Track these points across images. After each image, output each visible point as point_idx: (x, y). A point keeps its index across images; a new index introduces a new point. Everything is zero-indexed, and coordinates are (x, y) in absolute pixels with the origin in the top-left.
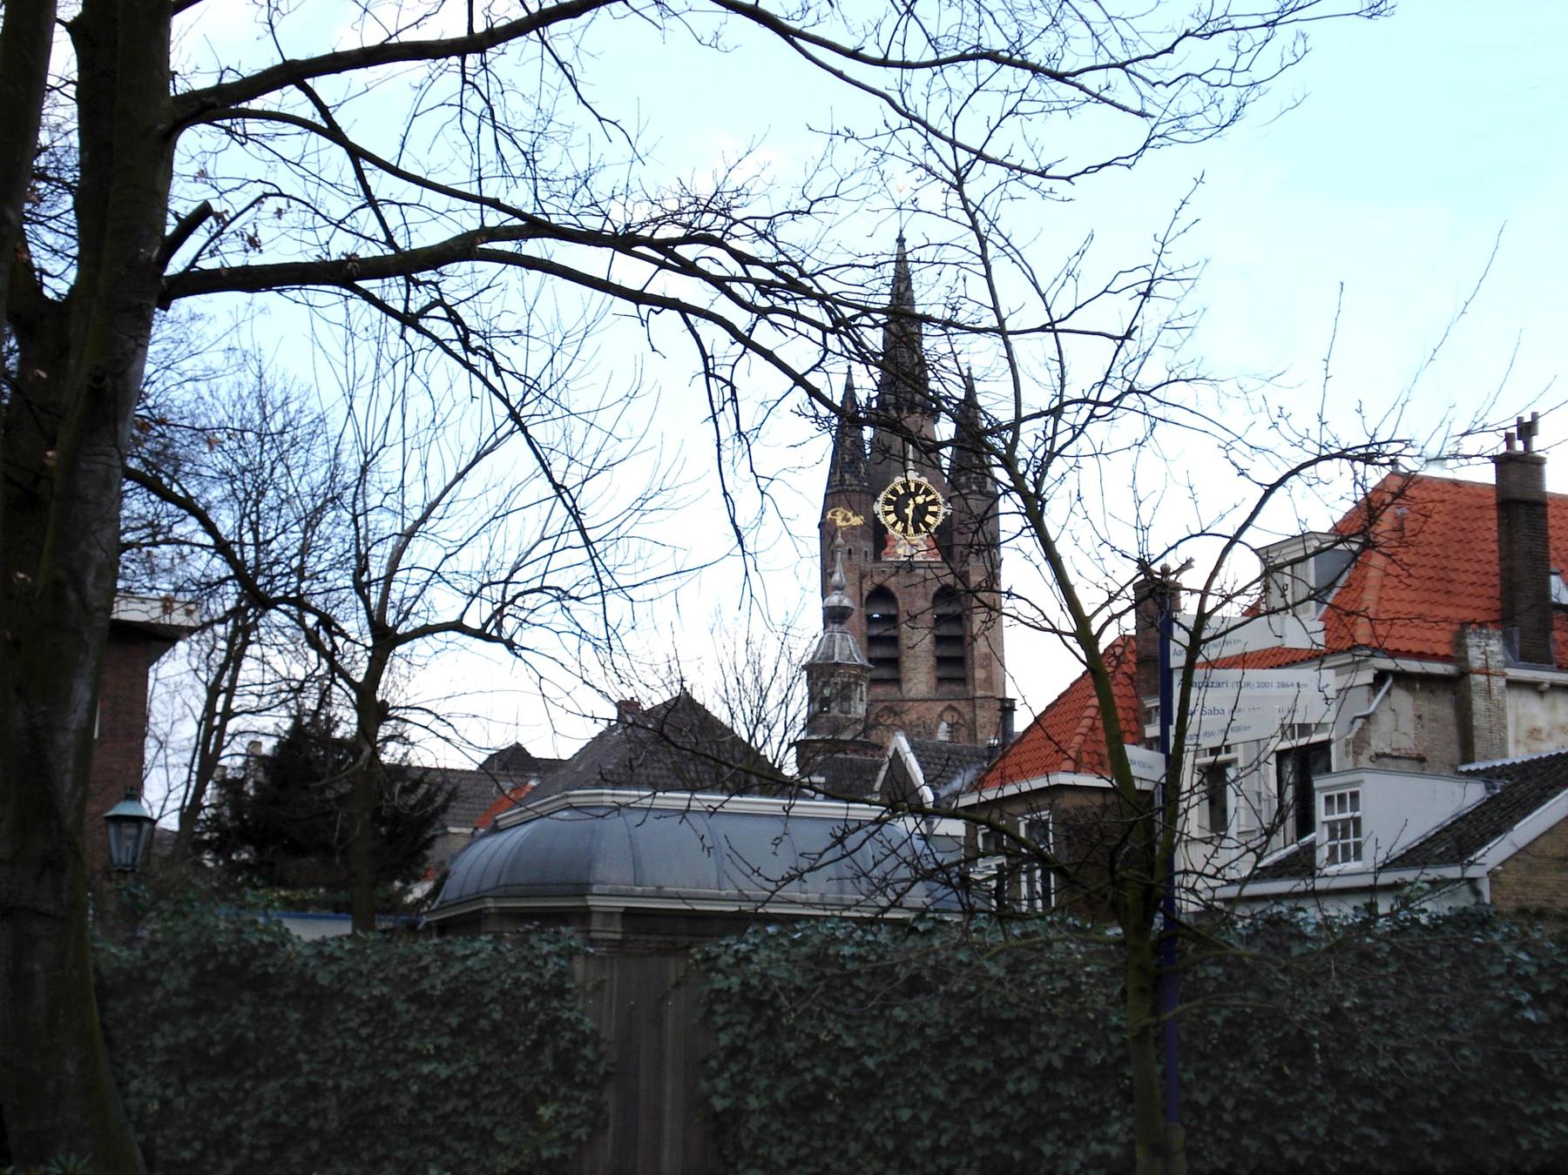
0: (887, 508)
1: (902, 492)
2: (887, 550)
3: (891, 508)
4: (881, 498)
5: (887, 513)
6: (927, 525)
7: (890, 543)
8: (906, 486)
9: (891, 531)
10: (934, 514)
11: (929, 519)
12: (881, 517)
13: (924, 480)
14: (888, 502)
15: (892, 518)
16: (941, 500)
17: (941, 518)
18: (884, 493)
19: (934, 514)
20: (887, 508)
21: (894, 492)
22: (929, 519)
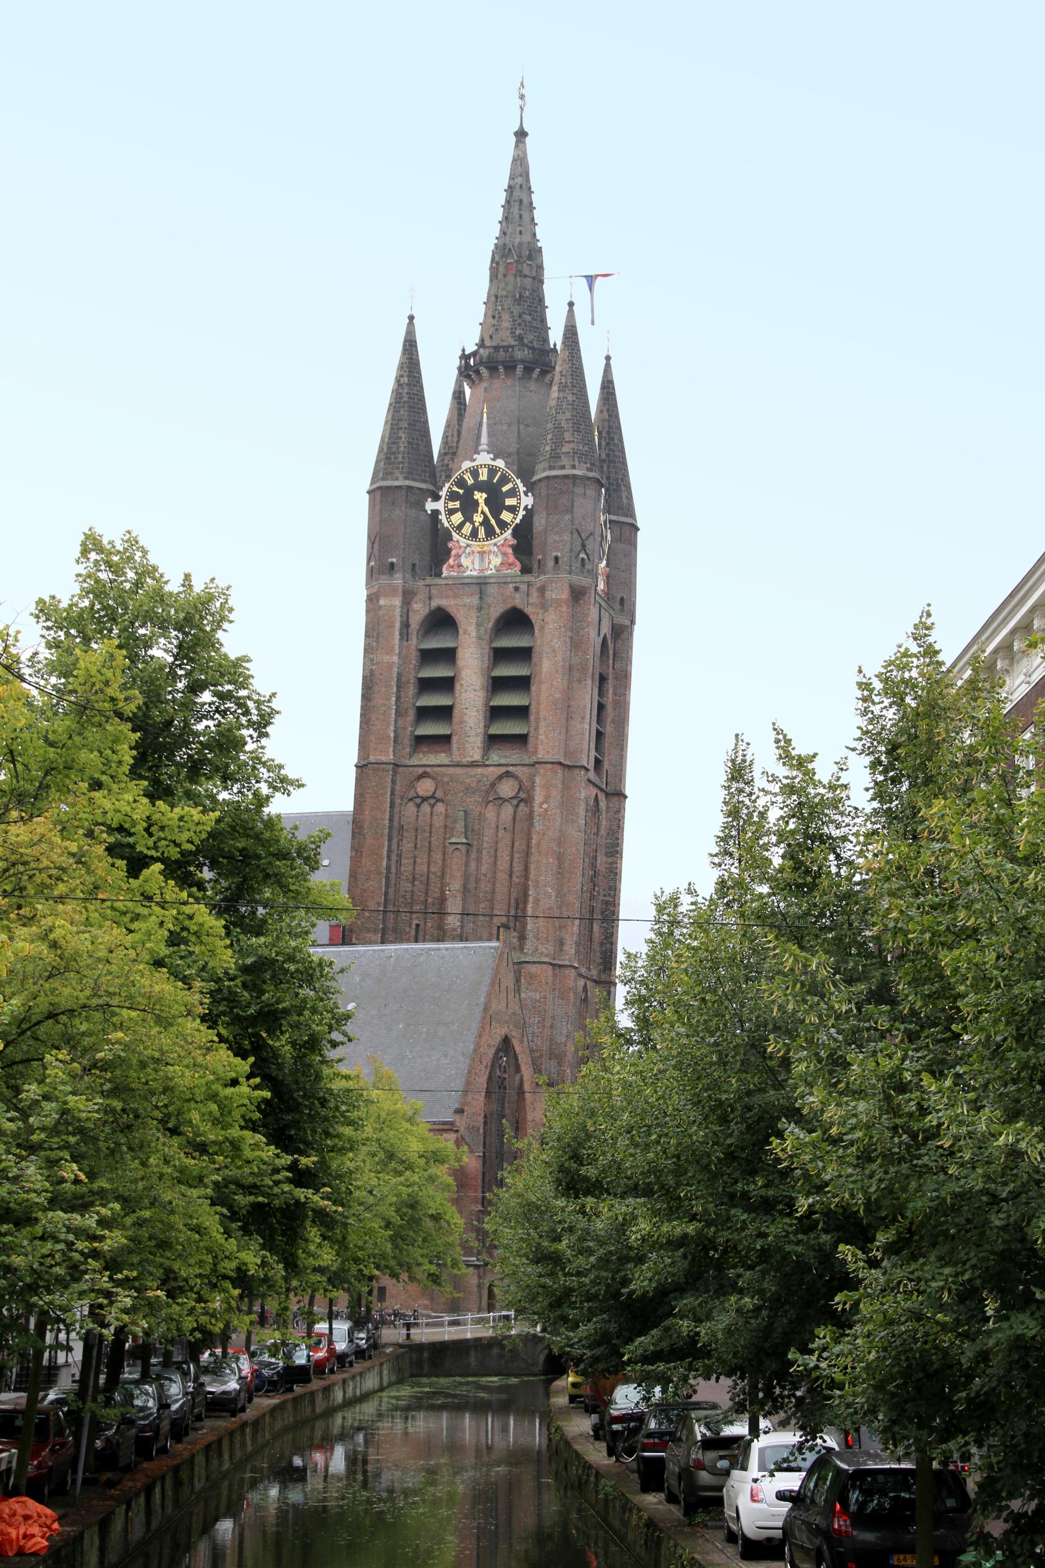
1: (470, 481)
2: (451, 561)
3: (457, 504)
4: (443, 493)
5: (451, 512)
6: (503, 525)
7: (453, 553)
8: (475, 473)
9: (455, 536)
10: (513, 509)
11: (506, 516)
12: (443, 517)
13: (500, 463)
14: (452, 496)
15: (458, 518)
16: (522, 488)
17: (522, 513)
18: (447, 485)
19: (513, 509)
21: (461, 483)
22: (506, 516)
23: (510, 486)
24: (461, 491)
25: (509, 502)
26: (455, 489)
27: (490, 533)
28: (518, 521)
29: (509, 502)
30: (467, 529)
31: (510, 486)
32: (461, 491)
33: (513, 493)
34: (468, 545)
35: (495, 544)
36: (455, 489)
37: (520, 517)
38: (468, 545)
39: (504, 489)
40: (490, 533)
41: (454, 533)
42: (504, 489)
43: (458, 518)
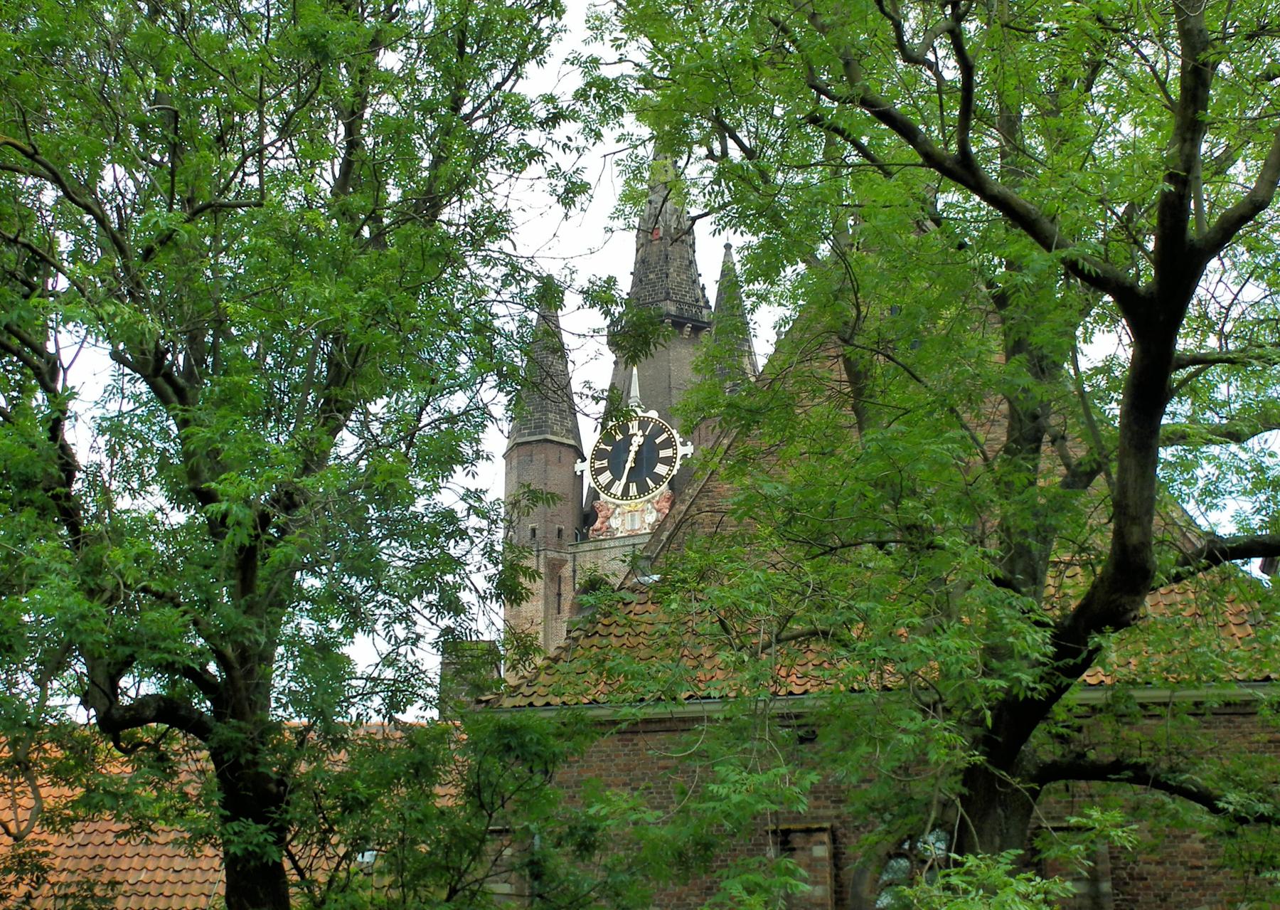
0: (598, 464)
2: (598, 525)
6: (658, 479)
10: (669, 461)
15: (606, 477)
16: (678, 439)
19: (669, 461)
20: (598, 464)
22: (661, 469)
23: (665, 436)
24: (609, 448)
25: (663, 453)
26: (602, 446)
27: (643, 490)
28: (675, 472)
29: (663, 453)
30: (618, 488)
31: (665, 436)
32: (609, 448)
33: (669, 443)
34: (618, 506)
35: (649, 501)
36: (602, 446)
37: (677, 466)
38: (618, 506)
39: (658, 441)
40: (643, 490)
41: (602, 495)
42: (658, 441)
43: (606, 477)
